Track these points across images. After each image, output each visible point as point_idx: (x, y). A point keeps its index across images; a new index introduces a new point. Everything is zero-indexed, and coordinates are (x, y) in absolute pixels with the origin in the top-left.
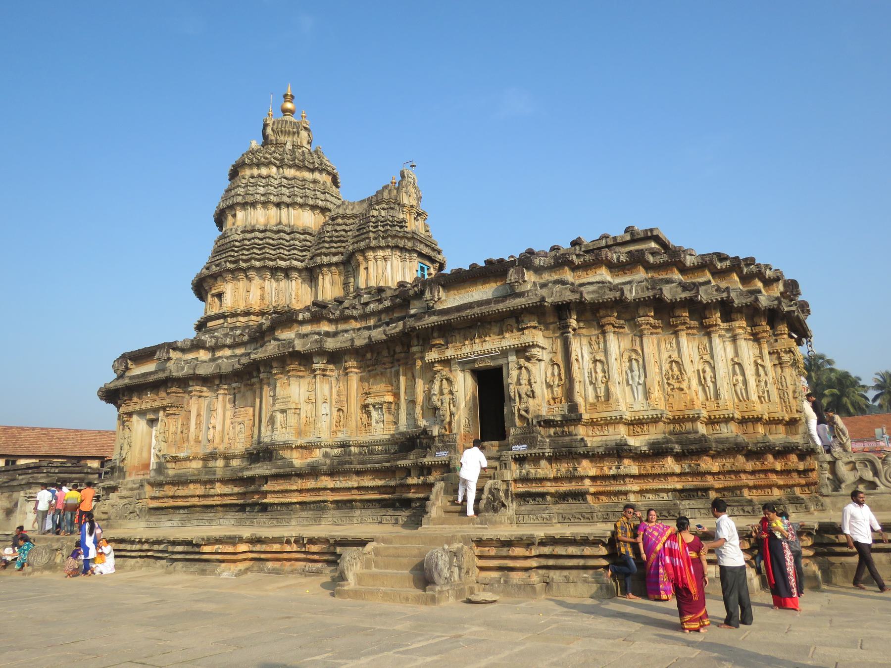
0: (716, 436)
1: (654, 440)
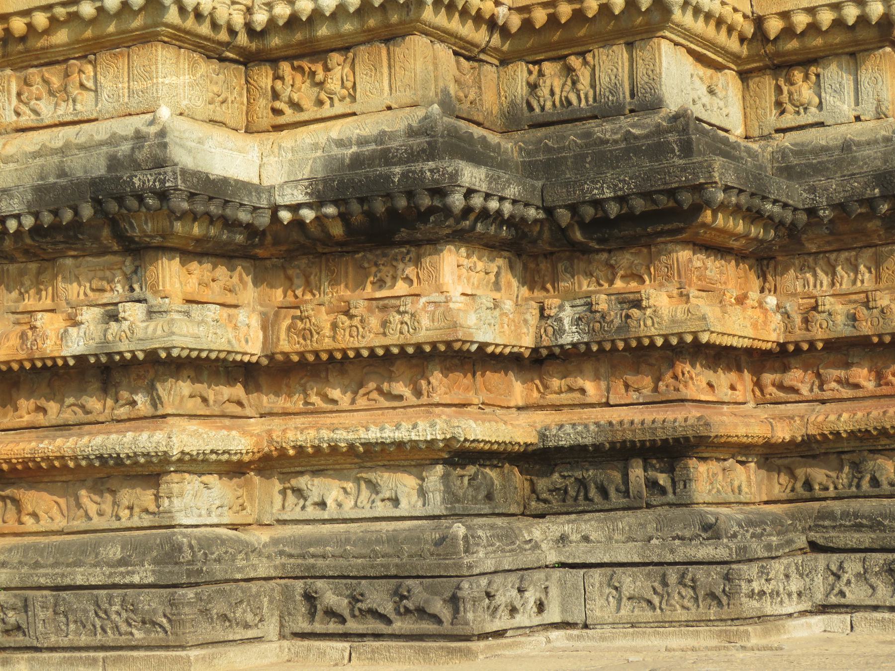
0: (787, 141)
1: (362, 142)
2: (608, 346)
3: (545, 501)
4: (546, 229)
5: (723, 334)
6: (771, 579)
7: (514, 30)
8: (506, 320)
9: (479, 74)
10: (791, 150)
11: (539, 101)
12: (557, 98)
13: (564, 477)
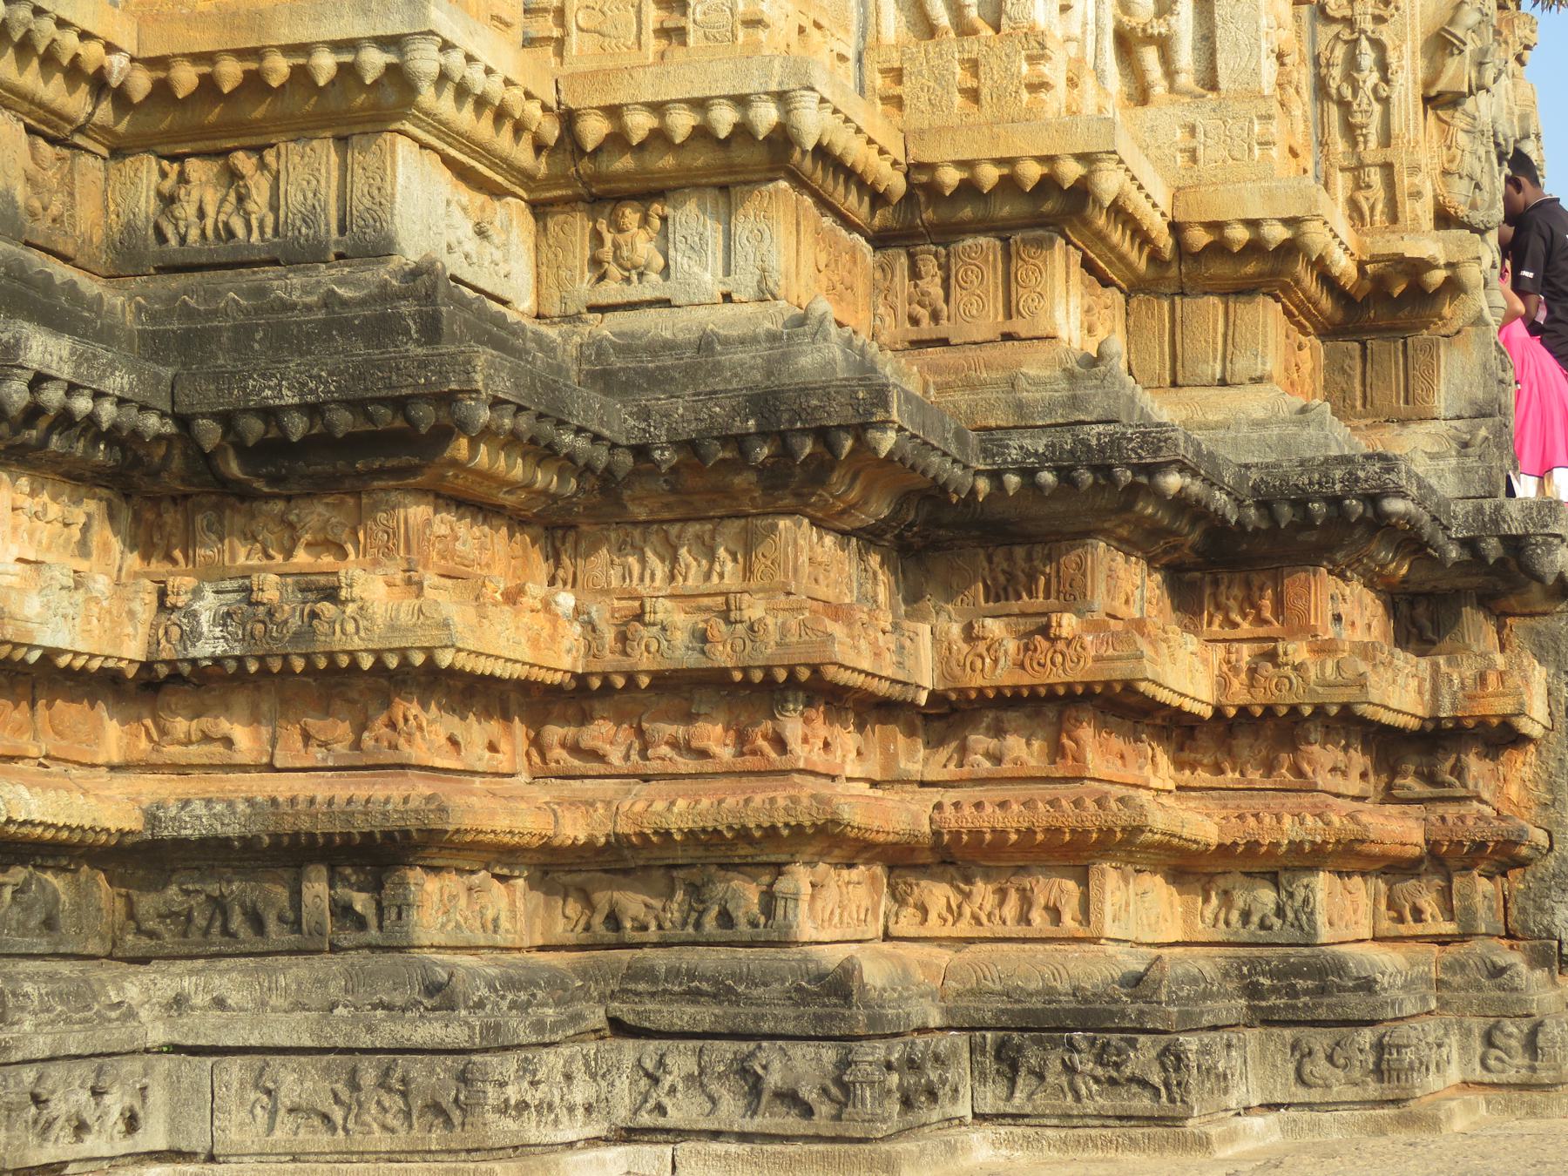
0: (606, 327)
2: (276, 665)
3: (152, 934)
4: (176, 452)
5: (479, 654)
6: (539, 1082)
7: (138, 96)
8: (95, 610)
9: (71, 170)
10: (613, 344)
11: (176, 227)
12: (209, 223)
13: (187, 893)
